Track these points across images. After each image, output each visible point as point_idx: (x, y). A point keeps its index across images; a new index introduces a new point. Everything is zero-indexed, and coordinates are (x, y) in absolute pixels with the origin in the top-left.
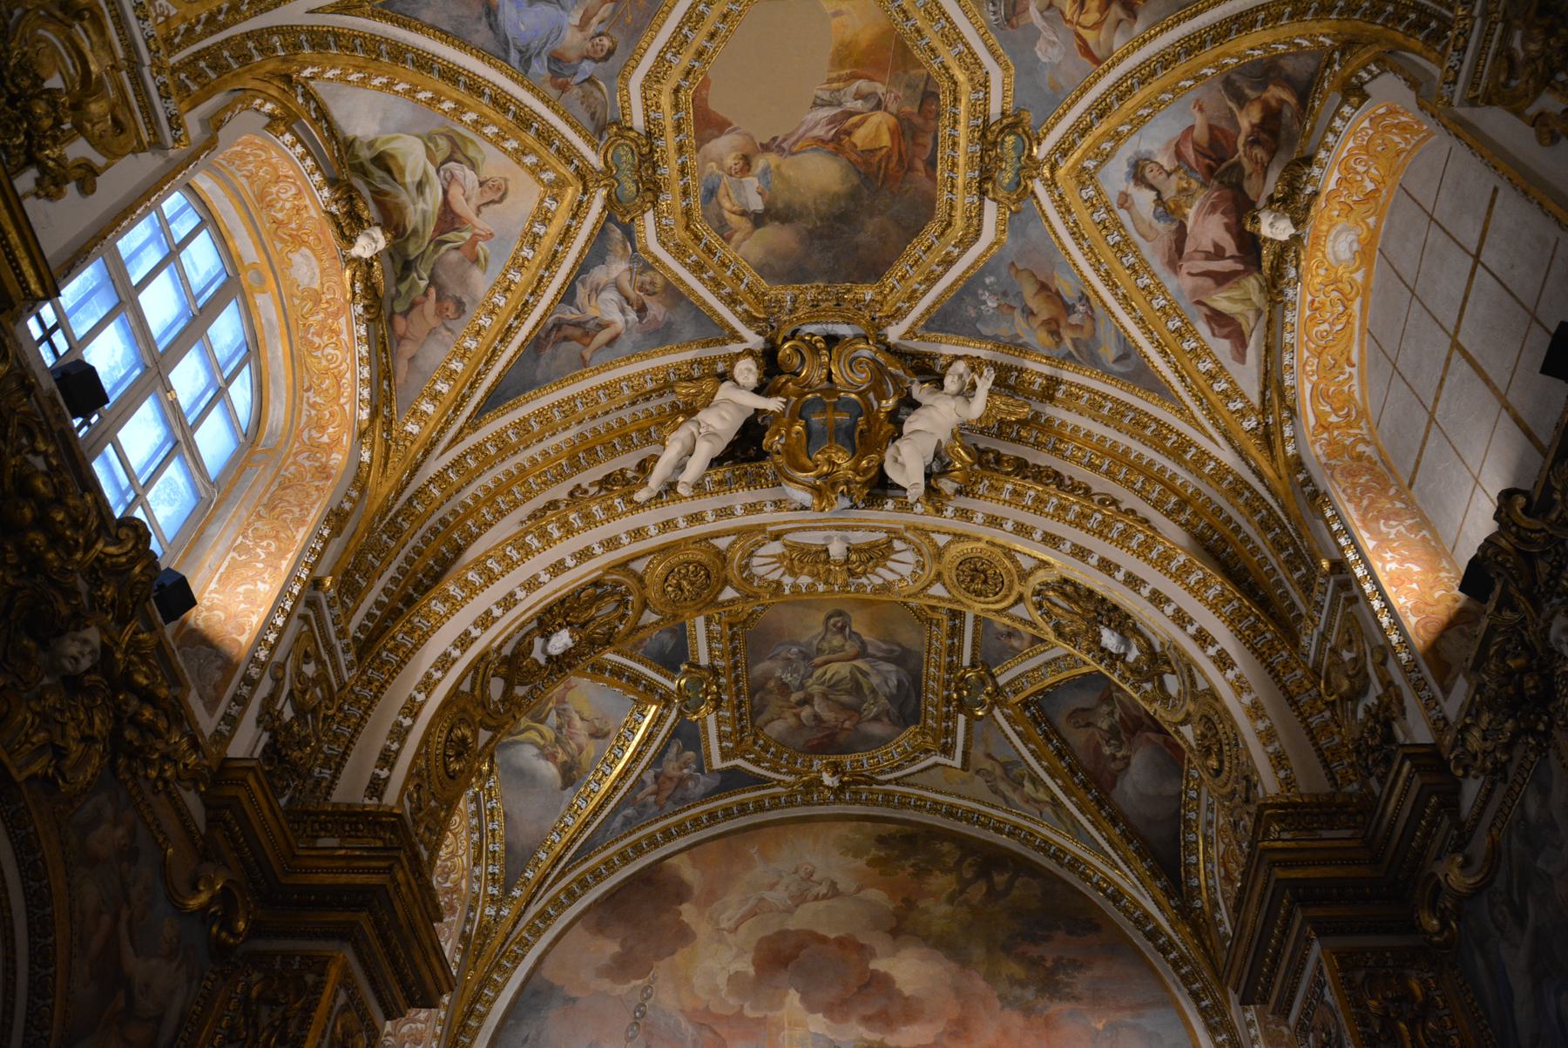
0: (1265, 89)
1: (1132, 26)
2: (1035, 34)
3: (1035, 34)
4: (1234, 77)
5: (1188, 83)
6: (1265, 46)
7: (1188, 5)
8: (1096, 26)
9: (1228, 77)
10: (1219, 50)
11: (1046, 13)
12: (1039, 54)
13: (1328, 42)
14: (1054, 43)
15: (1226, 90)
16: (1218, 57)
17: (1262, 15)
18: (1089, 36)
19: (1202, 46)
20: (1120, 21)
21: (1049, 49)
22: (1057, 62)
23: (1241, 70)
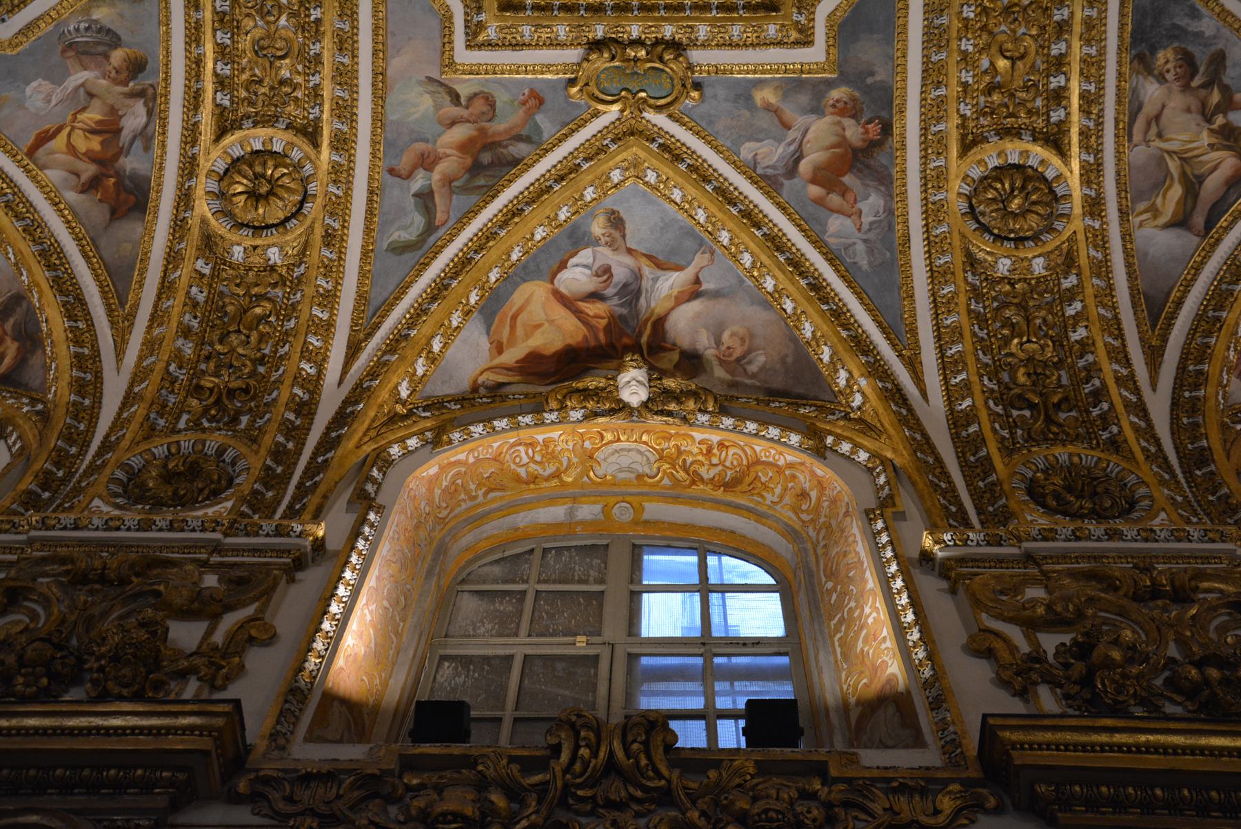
0: (14, 339)
1: (73, 189)
2: (57, 77)
3: (57, 77)
4: (25, 305)
5: (11, 255)
6: (50, 334)
7: (97, 247)
8: (71, 149)
9: (24, 298)
10: (45, 286)
11: (82, 90)
12: (34, 84)
13: (50, 396)
14: (49, 101)
15: (11, 297)
16: (38, 285)
17: (81, 325)
18: (60, 142)
19: (50, 267)
20: (77, 175)
21: (42, 96)
22: (28, 104)
23: (31, 311)
